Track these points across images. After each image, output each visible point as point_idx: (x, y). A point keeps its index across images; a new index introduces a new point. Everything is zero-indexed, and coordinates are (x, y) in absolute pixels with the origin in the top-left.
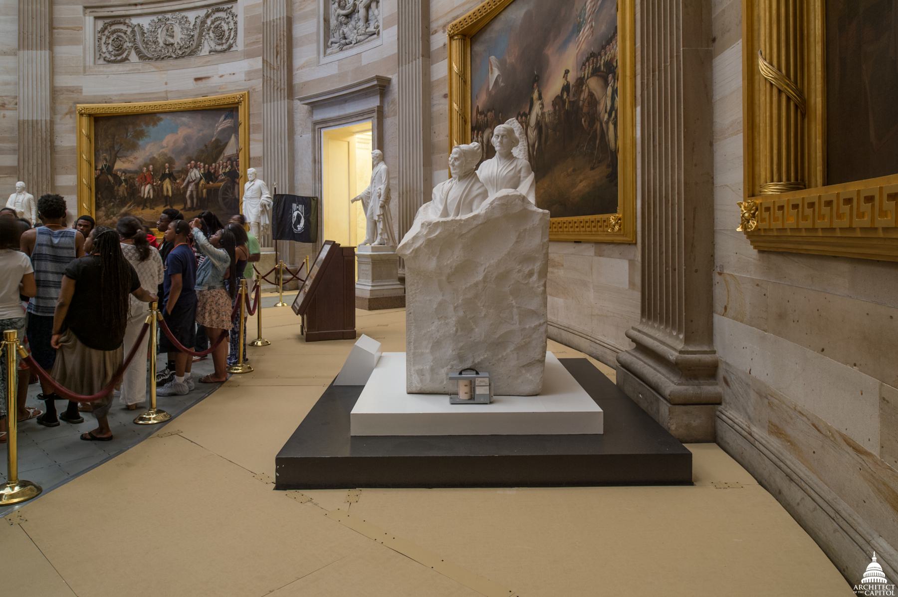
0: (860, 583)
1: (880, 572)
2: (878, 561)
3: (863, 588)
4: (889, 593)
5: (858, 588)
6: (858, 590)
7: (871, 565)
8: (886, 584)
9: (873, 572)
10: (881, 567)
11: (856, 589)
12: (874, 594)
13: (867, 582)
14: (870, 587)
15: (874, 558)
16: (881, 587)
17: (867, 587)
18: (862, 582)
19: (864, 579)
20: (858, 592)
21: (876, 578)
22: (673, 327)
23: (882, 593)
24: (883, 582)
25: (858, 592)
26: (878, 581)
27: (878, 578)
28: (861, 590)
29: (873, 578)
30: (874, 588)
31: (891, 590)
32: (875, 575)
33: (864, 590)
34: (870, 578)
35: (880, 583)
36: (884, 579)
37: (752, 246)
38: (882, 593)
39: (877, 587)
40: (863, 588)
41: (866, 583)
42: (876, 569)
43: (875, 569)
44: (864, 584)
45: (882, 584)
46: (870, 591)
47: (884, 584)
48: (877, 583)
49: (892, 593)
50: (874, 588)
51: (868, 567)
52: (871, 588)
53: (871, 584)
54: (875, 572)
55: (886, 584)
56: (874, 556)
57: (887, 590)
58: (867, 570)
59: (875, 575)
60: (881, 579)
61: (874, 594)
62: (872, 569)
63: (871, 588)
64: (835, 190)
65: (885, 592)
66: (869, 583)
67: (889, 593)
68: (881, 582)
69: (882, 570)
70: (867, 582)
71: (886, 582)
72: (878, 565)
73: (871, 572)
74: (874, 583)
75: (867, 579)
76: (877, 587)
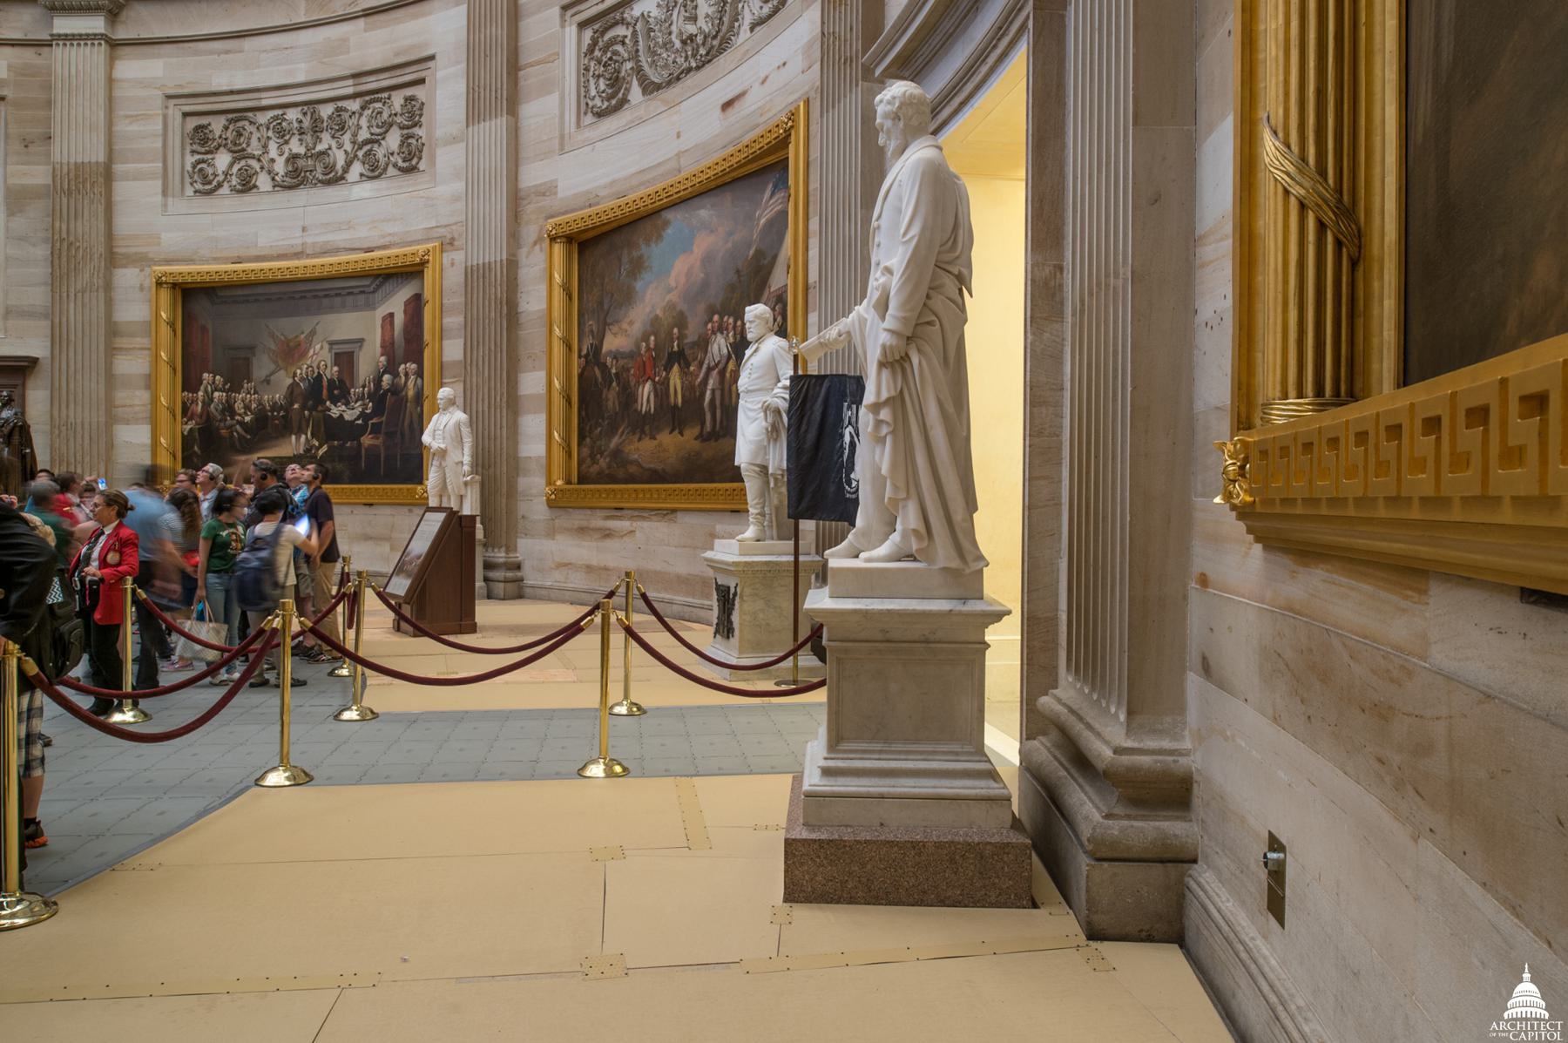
0: (1503, 1019)
1: (1536, 1000)
2: (1532, 981)
3: (1506, 1026)
4: (1552, 1036)
5: (1499, 1027)
6: (1497, 1032)
7: (1520, 988)
8: (1547, 1021)
9: (1524, 999)
10: (1538, 991)
11: (1494, 1029)
12: (1527, 1037)
13: (1515, 1016)
14: (1518, 1026)
15: (1527, 976)
16: (1539, 1025)
17: (1513, 1026)
18: (1506, 1017)
19: (1509, 1012)
20: (1497, 1035)
21: (1529, 1010)
22: (1085, 681)
23: (1540, 1035)
24: (1542, 1017)
25: (1497, 1035)
26: (1534, 1016)
27: (1534, 1010)
28: (1504, 1031)
29: (1524, 1010)
30: (1526, 1027)
31: (1556, 1031)
32: (1528, 1005)
33: (1509, 1032)
34: (1519, 1010)
35: (1536, 1019)
36: (1544, 1012)
37: (1252, 536)
38: (1540, 1035)
39: (1532, 1026)
40: (1506, 1026)
41: (1513, 1019)
42: (1530, 994)
43: (1527, 994)
44: (1507, 1021)
45: (1539, 1020)
46: (1520, 1032)
47: (1544, 1020)
48: (1531, 1019)
49: (1557, 1036)
50: (1526, 1027)
51: (1515, 991)
52: (1521, 1028)
53: (1521, 1020)
54: (1528, 999)
55: (1547, 1021)
56: (1526, 971)
57: (1548, 1031)
58: (1514, 995)
59: (1528, 1005)
60: (1539, 1011)
61: (1527, 1037)
62: (1523, 994)
63: (1521, 1028)
64: (1431, 393)
65: (1546, 1035)
66: (1516, 1019)
67: (1552, 1036)
68: (1538, 1016)
69: (1539, 995)
70: (1515, 1016)
71: (1547, 1017)
72: (1533, 988)
73: (1521, 999)
74: (1526, 1019)
75: (1514, 1011)
76: (1532, 1026)
